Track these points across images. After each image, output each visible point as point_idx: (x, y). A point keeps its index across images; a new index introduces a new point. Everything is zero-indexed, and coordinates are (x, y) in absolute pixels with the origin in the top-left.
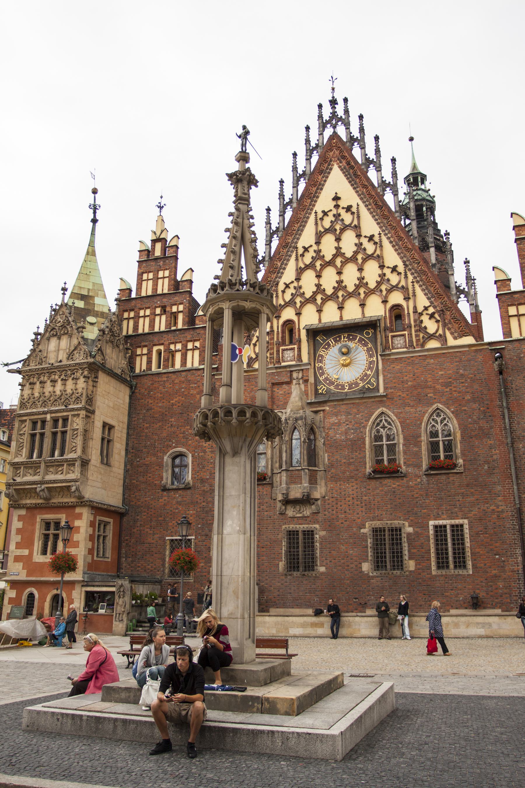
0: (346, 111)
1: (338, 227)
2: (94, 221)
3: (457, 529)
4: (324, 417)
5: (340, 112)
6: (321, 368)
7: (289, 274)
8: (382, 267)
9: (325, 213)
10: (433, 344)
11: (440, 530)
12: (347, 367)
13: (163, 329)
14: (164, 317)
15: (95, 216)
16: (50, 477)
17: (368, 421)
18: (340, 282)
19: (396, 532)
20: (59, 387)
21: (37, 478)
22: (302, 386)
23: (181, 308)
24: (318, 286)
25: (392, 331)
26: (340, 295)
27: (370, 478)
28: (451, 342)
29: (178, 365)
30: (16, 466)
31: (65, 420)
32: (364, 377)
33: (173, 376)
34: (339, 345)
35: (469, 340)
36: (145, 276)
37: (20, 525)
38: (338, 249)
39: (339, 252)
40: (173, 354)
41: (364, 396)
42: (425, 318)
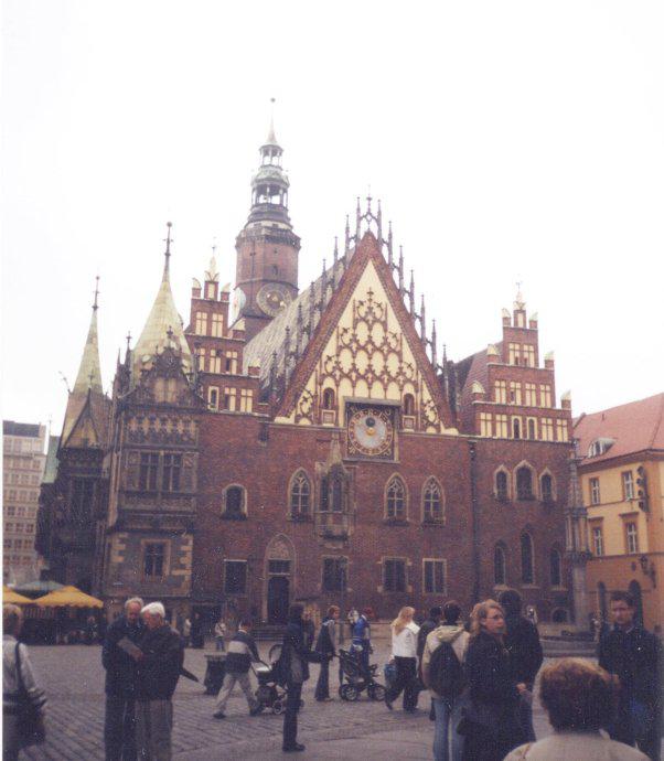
0: (379, 213)
1: (370, 318)
2: (168, 255)
3: (441, 563)
4: (355, 474)
5: (375, 214)
6: (352, 433)
7: (330, 349)
8: (401, 361)
9: (362, 303)
10: (431, 430)
11: (429, 565)
12: (371, 437)
13: (218, 371)
14: (218, 361)
15: (168, 250)
16: (165, 507)
17: (386, 481)
18: (370, 366)
19: (400, 565)
20: (169, 427)
21: (149, 507)
22: (339, 446)
23: (235, 355)
24: (354, 365)
25: (406, 413)
26: (369, 377)
27: (386, 524)
28: (444, 431)
29: (232, 408)
30: (129, 494)
31: (178, 458)
32: (383, 446)
33: (231, 418)
34: (366, 417)
35: (453, 432)
36: (199, 315)
37: (123, 547)
38: (370, 337)
39: (370, 341)
40: (228, 397)
41: (379, 464)
42: (427, 409)
